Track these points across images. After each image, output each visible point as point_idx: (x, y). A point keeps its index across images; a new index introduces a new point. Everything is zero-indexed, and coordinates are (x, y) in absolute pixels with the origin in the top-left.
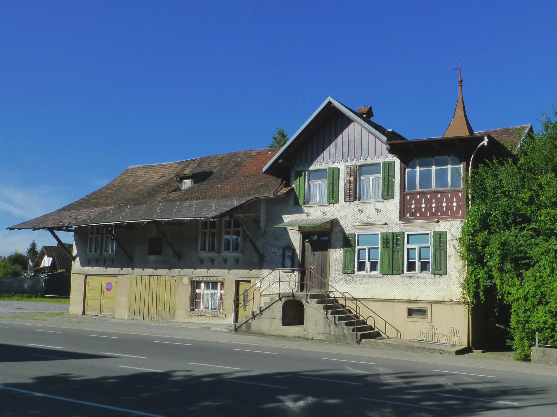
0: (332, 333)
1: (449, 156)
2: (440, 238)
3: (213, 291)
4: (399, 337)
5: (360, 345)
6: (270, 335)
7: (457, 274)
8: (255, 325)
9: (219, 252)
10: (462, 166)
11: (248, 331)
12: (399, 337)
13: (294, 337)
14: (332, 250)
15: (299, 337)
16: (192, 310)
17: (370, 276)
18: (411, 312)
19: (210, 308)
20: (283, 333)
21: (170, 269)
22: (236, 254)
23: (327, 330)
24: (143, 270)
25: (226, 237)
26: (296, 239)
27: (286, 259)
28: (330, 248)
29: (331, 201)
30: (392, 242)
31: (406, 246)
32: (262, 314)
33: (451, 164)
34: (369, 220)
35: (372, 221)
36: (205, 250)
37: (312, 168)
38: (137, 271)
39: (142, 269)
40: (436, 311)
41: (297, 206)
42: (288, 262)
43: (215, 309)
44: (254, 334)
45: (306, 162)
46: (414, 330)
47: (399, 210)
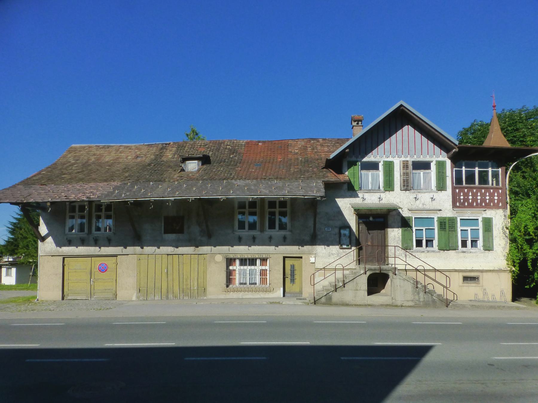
0: (422, 300)
1: (490, 161)
2: (488, 224)
3: (253, 267)
4: (456, 299)
5: (449, 308)
6: (355, 305)
7: (502, 250)
8: (336, 297)
9: (262, 230)
10: (500, 170)
11: (329, 302)
12: (456, 299)
13: (382, 305)
14: (390, 230)
15: (387, 305)
16: (227, 286)
17: (428, 252)
18: (466, 279)
19: (248, 283)
20: (369, 302)
21: (197, 247)
22: (283, 233)
23: (417, 297)
24: (159, 248)
25: (240, 217)
26: (352, 220)
27: (340, 235)
28: (388, 227)
29: (388, 189)
30: (446, 225)
31: (469, 229)
32: (344, 287)
33: (492, 168)
34: (425, 206)
35: (427, 207)
36: (244, 228)
37: (366, 159)
38: (148, 249)
39: (156, 248)
40: (485, 278)
41: (351, 192)
42: (345, 240)
43: (245, 284)
44: (336, 304)
45: (360, 154)
46: (466, 293)
47: (451, 200)
